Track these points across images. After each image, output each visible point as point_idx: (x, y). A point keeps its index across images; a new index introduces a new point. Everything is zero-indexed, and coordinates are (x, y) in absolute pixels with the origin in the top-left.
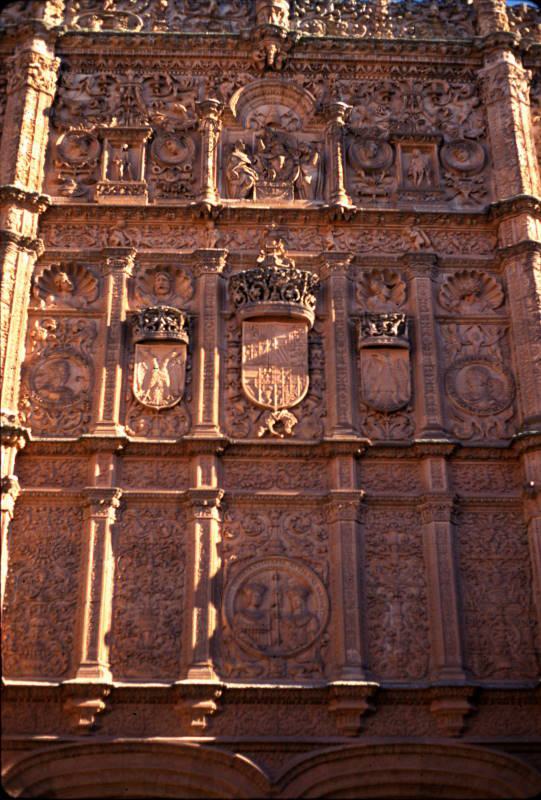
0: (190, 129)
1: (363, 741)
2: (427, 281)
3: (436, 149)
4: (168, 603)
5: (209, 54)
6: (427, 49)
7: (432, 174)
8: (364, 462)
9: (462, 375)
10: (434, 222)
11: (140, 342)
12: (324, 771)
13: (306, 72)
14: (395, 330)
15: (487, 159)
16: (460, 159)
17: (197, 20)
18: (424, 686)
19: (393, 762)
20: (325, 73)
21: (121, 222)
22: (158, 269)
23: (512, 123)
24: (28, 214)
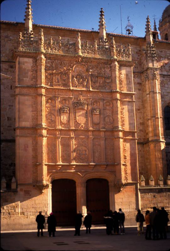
1: (93, 171)
2: (102, 103)
9: (106, 118)
12: (88, 175)
13: (84, 62)
17: (66, 49)
19: (96, 173)
21: (57, 91)
22: (64, 100)
23: (116, 76)
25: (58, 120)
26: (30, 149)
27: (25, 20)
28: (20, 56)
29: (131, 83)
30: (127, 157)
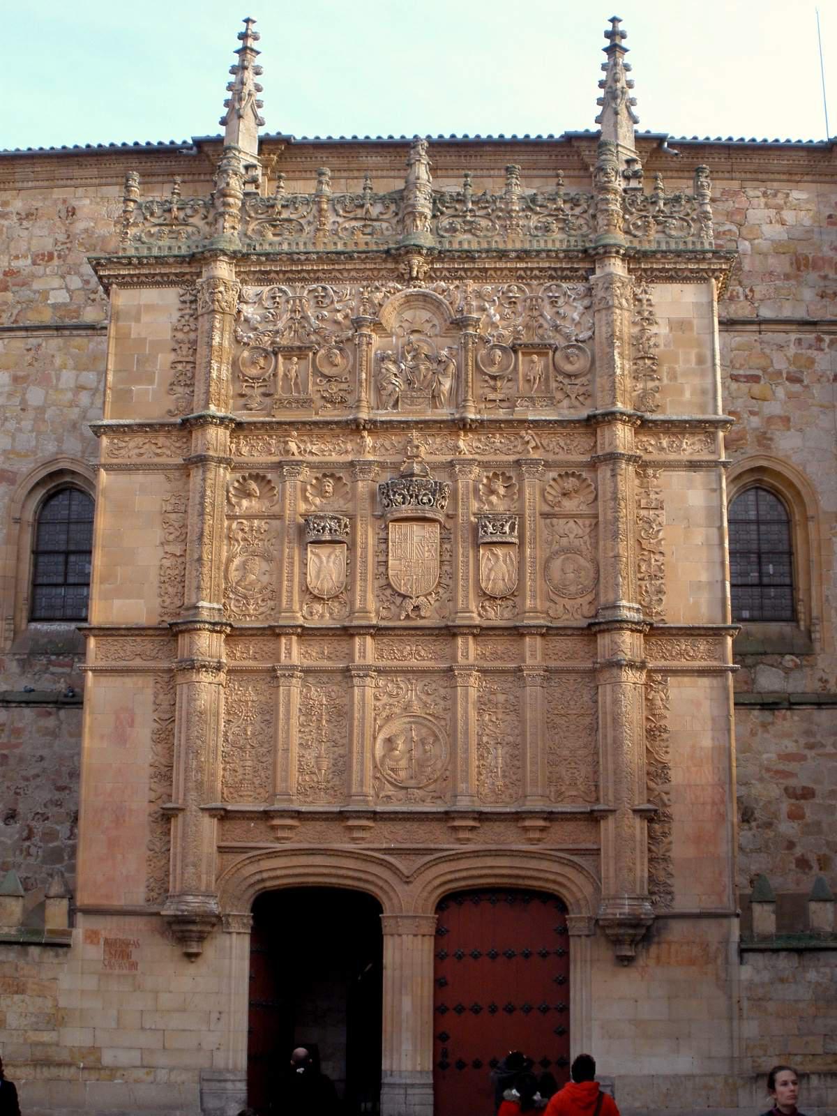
0: (348, 340)
3: (551, 353)
4: (336, 749)
5: (363, 266)
6: (548, 256)
7: (547, 379)
8: (480, 638)
9: (557, 564)
10: (543, 426)
11: (311, 543)
12: (444, 867)
13: (444, 279)
14: (507, 529)
15: (593, 362)
16: (571, 363)
17: (354, 223)
18: (513, 810)
19: (490, 862)
20: (461, 278)
22: (325, 476)
23: (613, 335)
24: (221, 431)
25: (291, 580)
26: (143, 733)
27: (224, 122)
28: (117, 284)
29: (709, 364)
30: (672, 773)
